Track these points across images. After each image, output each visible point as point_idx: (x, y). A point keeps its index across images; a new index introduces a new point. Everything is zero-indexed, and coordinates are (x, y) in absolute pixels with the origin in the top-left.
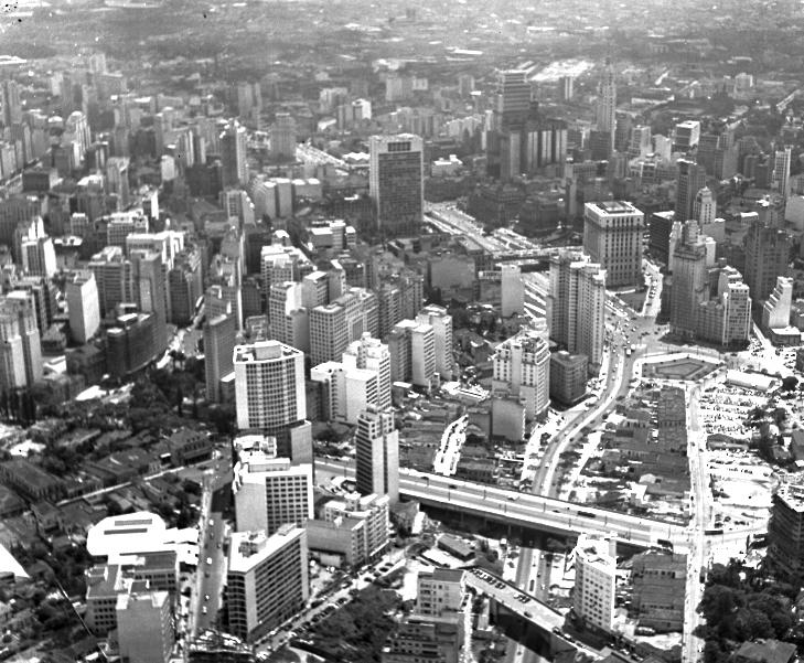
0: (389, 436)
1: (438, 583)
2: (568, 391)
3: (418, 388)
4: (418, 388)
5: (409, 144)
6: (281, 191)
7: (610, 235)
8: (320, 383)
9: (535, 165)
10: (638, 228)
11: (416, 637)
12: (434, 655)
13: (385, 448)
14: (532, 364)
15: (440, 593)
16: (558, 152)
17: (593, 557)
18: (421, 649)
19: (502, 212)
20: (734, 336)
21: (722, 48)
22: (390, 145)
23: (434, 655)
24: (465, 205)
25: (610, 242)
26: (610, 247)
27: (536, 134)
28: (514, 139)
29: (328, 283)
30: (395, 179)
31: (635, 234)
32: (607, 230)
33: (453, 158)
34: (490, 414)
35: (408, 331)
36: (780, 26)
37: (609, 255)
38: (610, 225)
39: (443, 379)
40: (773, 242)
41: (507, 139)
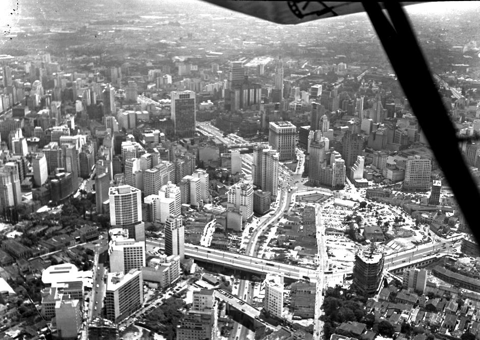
0: (180, 229)
1: (202, 296)
2: (262, 208)
3: (193, 207)
4: (193, 207)
5: (189, 95)
6: (130, 116)
7: (281, 137)
8: (148, 205)
9: (247, 104)
10: (294, 134)
11: (193, 321)
12: (200, 329)
13: (178, 234)
14: (245, 196)
15: (203, 301)
16: (257, 99)
17: (273, 284)
18: (195, 326)
19: (232, 126)
20: (338, 183)
21: (332, 51)
22: (180, 95)
23: (200, 329)
24: (215, 123)
25: (281, 140)
26: (281, 143)
27: (247, 90)
28: (237, 93)
29: (152, 159)
30: (183, 111)
31: (292, 137)
32: (280, 134)
33: (209, 101)
34: (226, 218)
35: (189, 180)
36: (359, 41)
37: (281, 146)
38: (281, 132)
39: (205, 203)
40: (355, 140)
41: (234, 93)
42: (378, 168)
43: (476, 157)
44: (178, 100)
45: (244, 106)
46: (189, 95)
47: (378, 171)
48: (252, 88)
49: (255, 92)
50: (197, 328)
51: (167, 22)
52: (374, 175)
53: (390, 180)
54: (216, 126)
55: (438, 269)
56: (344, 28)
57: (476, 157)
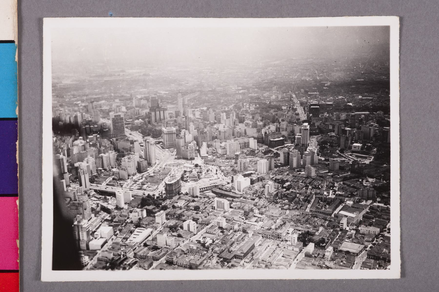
0: (86, 175)
1: (81, 196)
2: (142, 169)
3: (105, 170)
4: (105, 170)
5: (120, 115)
6: (87, 129)
7: (167, 136)
8: (76, 167)
9: (159, 120)
10: (175, 133)
11: (74, 206)
12: (78, 209)
13: (85, 178)
14: (130, 162)
15: (82, 199)
16: (165, 117)
17: (118, 193)
18: (75, 208)
19: (148, 132)
20: (191, 157)
21: (353, 86)
22: (115, 116)
23: (78, 209)
24: (140, 132)
25: (167, 137)
26: (167, 138)
27: (159, 112)
28: (153, 114)
29: (85, 146)
30: (117, 124)
31: (174, 135)
32: (166, 134)
33: (140, 120)
34: (119, 173)
35: (102, 156)
36: (262, 81)
37: (167, 140)
38: (167, 133)
39: (112, 168)
40: (203, 134)
41: (151, 114)
42: (216, 149)
43: (269, 141)
44: (114, 118)
45: (157, 121)
46: (120, 115)
47: (215, 150)
48: (162, 111)
49: (164, 112)
50: (76, 209)
51: (142, 74)
52: (212, 152)
53: (220, 154)
54: (141, 133)
55: (214, 190)
56: (259, 73)
57: (269, 141)
